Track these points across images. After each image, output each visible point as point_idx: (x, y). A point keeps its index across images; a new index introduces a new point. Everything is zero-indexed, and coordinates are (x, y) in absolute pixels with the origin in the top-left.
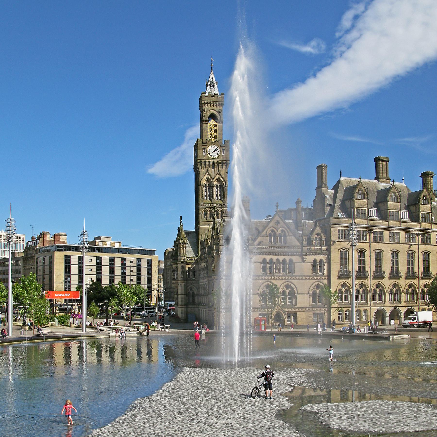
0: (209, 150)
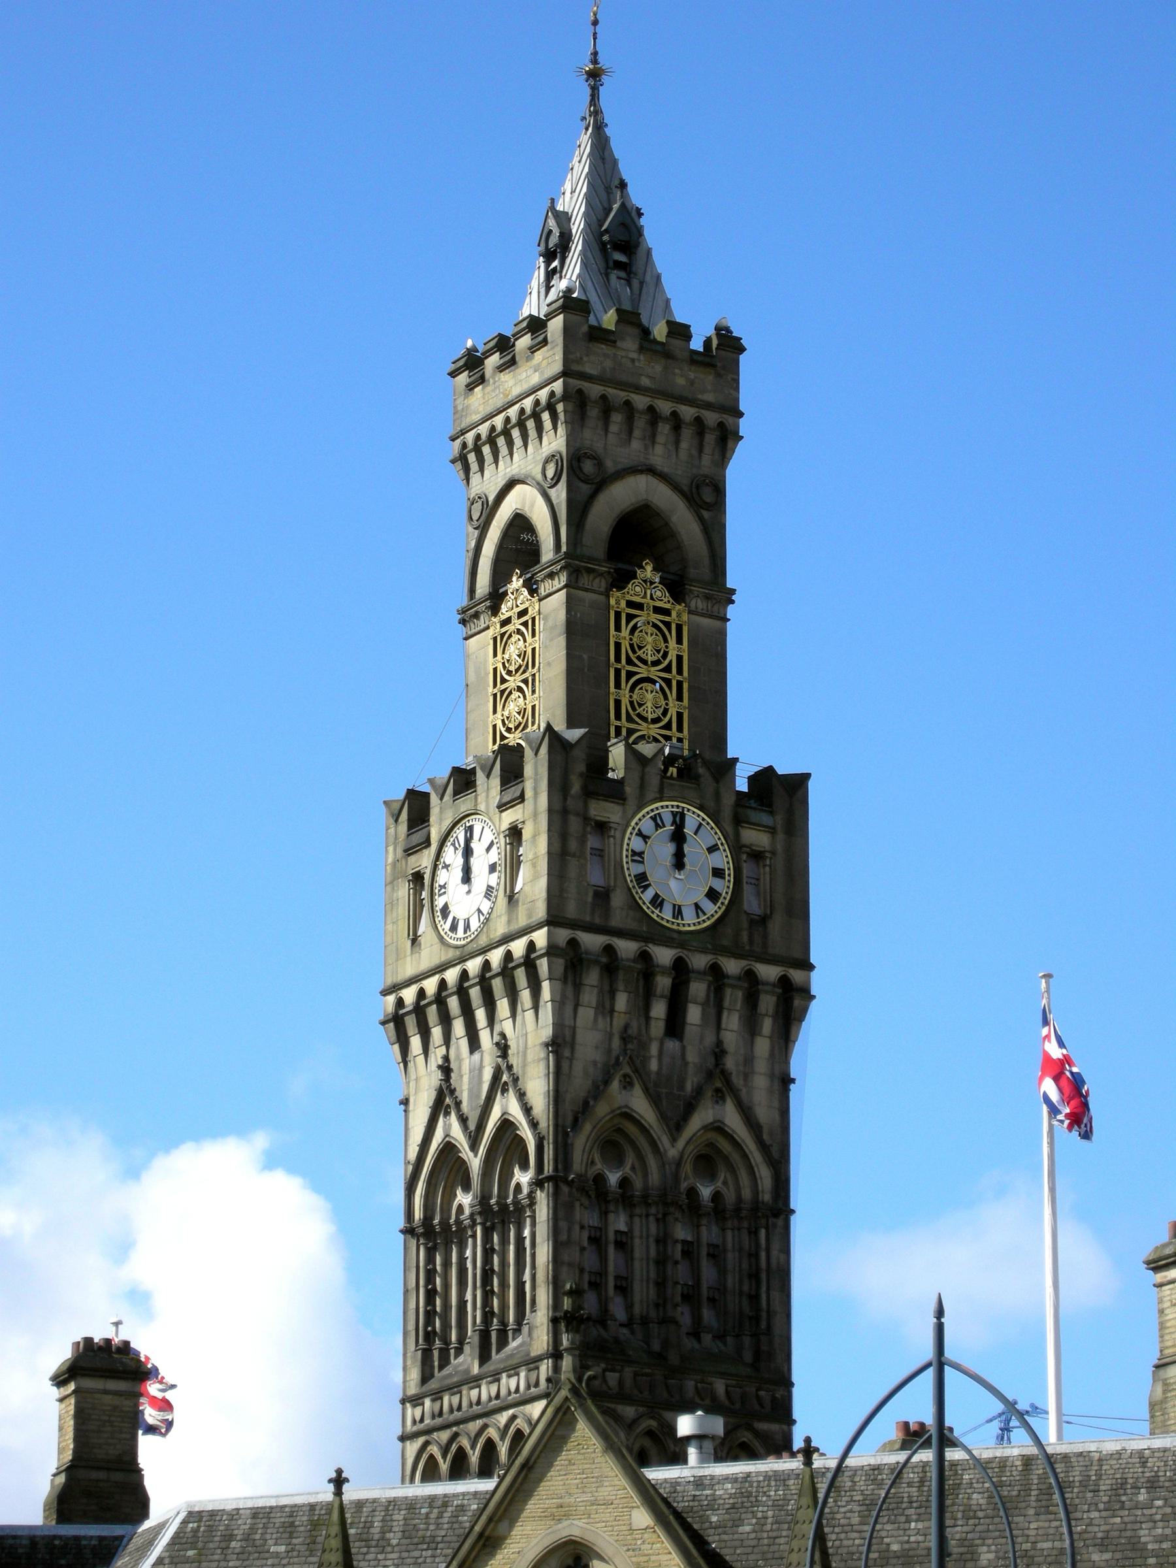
0: (637, 844)
